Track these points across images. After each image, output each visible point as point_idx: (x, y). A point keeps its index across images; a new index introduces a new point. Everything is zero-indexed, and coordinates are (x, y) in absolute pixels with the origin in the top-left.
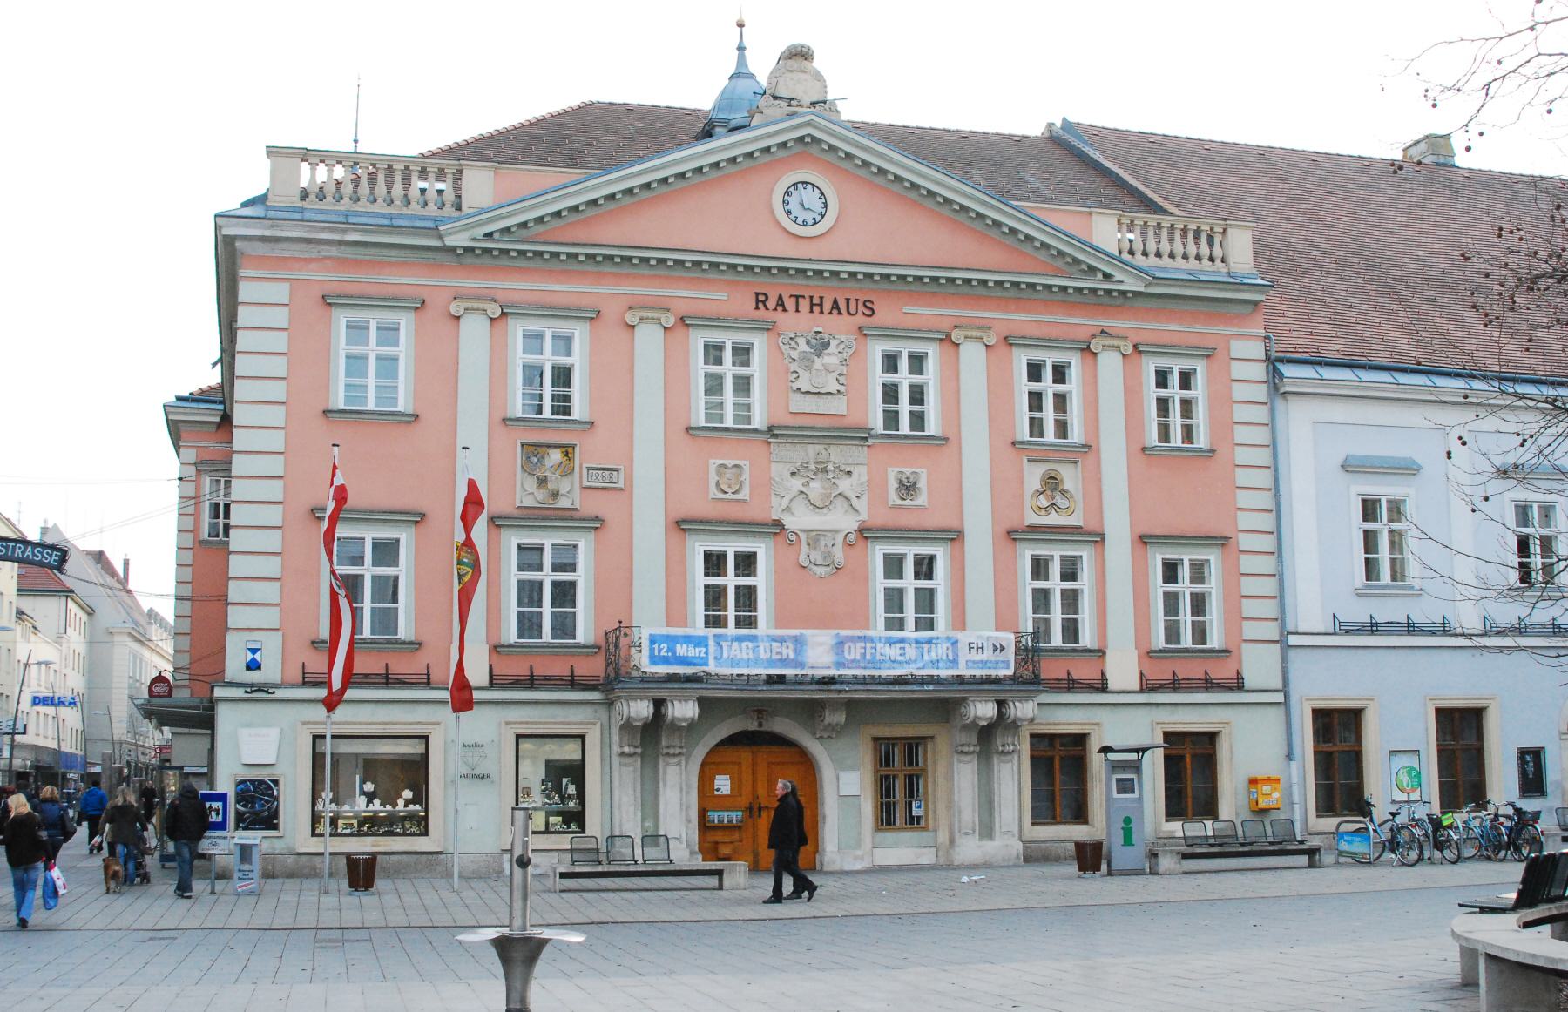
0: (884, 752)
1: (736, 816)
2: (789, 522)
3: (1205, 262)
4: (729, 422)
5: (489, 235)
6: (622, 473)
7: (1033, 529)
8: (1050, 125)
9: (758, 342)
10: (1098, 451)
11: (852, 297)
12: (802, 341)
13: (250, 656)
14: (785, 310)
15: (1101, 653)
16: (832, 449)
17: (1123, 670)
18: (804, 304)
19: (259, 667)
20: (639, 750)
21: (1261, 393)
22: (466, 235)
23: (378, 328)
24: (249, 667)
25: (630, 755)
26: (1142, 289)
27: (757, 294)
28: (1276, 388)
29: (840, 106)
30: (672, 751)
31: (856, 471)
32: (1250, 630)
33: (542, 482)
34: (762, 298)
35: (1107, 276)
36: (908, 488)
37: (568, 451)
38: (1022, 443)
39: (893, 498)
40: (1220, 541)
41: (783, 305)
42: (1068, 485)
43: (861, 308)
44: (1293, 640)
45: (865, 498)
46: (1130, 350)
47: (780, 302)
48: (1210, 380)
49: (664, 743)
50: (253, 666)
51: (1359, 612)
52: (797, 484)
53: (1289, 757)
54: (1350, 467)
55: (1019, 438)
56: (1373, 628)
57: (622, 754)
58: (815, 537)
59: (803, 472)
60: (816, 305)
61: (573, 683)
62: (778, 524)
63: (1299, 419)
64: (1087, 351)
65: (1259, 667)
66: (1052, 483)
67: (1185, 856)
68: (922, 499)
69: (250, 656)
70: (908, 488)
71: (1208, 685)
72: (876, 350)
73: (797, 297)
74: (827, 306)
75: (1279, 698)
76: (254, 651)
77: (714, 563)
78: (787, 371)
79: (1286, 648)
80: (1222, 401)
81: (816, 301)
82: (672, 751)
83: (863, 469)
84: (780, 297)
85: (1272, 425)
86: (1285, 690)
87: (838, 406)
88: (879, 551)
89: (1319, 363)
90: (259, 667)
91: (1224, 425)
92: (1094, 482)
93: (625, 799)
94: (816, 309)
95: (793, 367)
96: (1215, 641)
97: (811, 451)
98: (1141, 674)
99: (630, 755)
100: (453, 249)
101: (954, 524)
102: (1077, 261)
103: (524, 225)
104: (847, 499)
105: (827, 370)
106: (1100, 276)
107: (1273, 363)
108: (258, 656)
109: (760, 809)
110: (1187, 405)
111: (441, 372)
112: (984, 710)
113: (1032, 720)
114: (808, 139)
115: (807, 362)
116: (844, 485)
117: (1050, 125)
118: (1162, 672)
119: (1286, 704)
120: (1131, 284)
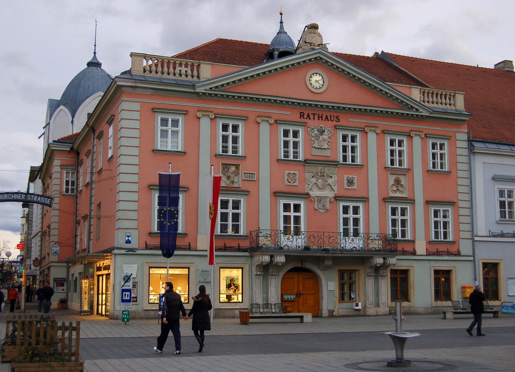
0: (341, 274)
1: (293, 297)
2: (311, 193)
3: (448, 105)
4: (291, 158)
5: (211, 88)
6: (256, 175)
7: (392, 198)
8: (376, 53)
9: (301, 131)
10: (413, 171)
11: (332, 115)
12: (316, 130)
13: (127, 238)
14: (310, 119)
15: (413, 242)
16: (326, 168)
17: (421, 248)
18: (316, 117)
19: (130, 242)
20: (262, 273)
21: (466, 152)
22: (203, 88)
23: (172, 121)
24: (127, 242)
25: (259, 275)
26: (428, 115)
27: (301, 113)
28: (471, 150)
29: (328, 46)
30: (273, 274)
31: (334, 176)
33: (228, 177)
34: (302, 114)
35: (417, 110)
36: (350, 182)
37: (237, 166)
38: (389, 168)
39: (346, 186)
40: (452, 203)
41: (309, 117)
42: (403, 183)
43: (335, 119)
44: (476, 239)
45: (336, 186)
46: (423, 136)
47: (308, 116)
48: (449, 147)
49: (271, 271)
50: (128, 242)
51: (497, 229)
52: (314, 180)
53: (475, 279)
54: (495, 179)
55: (387, 166)
56: (502, 235)
57: (257, 275)
58: (320, 199)
59: (316, 176)
60: (320, 117)
61: (239, 249)
62: (308, 194)
63: (479, 162)
64: (410, 137)
65: (465, 247)
66: (397, 182)
67: (455, 313)
68: (355, 187)
69: (127, 238)
70: (350, 182)
71: (449, 253)
72: (340, 134)
73: (314, 114)
74: (324, 118)
75: (472, 258)
76: (128, 236)
77: (287, 207)
78: (311, 140)
79: (474, 241)
80: (453, 155)
81: (320, 116)
82: (273, 274)
83: (336, 176)
84: (308, 114)
85: (470, 163)
86: (474, 256)
87: (328, 153)
88: (341, 204)
89: (485, 142)
90: (130, 242)
91: (454, 163)
93: (257, 291)
94: (320, 119)
95: (313, 139)
96: (450, 238)
97: (320, 168)
98: (427, 249)
99: (259, 275)
100: (198, 93)
101: (366, 196)
102: (407, 104)
103: (223, 85)
104: (331, 186)
105: (324, 140)
106: (414, 110)
107: (470, 141)
108: (130, 238)
109: (300, 294)
110: (400, 153)
111: (193, 138)
112: (379, 261)
113: (394, 265)
114: (318, 58)
115: (317, 137)
116: (330, 181)
117: (376, 53)
118: (433, 249)
119: (474, 261)
120: (425, 113)
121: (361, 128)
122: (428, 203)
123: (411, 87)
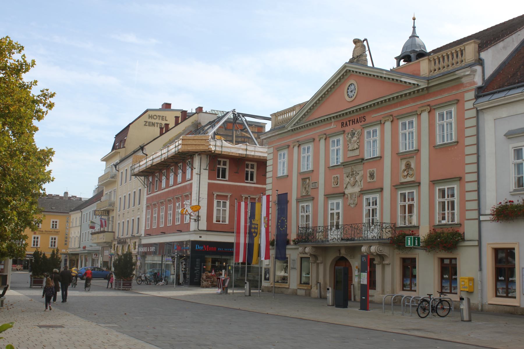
2: (347, 192)
5: (295, 124)
7: (402, 184)
15: (418, 227)
18: (351, 122)
31: (360, 172)
32: (469, 215)
39: (369, 180)
42: (413, 166)
52: (348, 179)
58: (351, 194)
60: (353, 122)
65: (470, 231)
66: (408, 166)
68: (375, 180)
73: (349, 121)
83: (362, 172)
87: (357, 153)
92: (418, 164)
100: (289, 131)
103: (300, 119)
116: (358, 178)
119: (480, 245)
121: (377, 121)
122: (434, 182)
123: (419, 62)
